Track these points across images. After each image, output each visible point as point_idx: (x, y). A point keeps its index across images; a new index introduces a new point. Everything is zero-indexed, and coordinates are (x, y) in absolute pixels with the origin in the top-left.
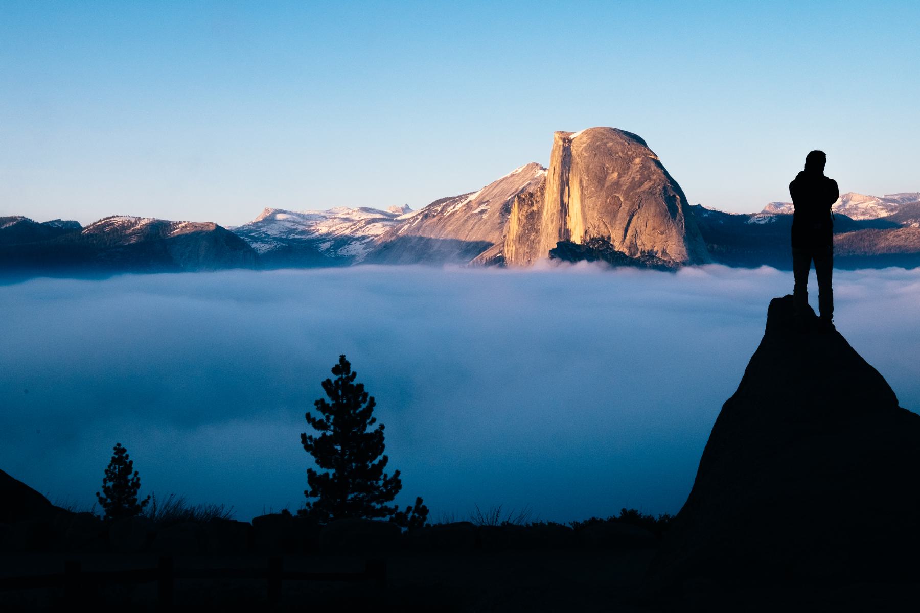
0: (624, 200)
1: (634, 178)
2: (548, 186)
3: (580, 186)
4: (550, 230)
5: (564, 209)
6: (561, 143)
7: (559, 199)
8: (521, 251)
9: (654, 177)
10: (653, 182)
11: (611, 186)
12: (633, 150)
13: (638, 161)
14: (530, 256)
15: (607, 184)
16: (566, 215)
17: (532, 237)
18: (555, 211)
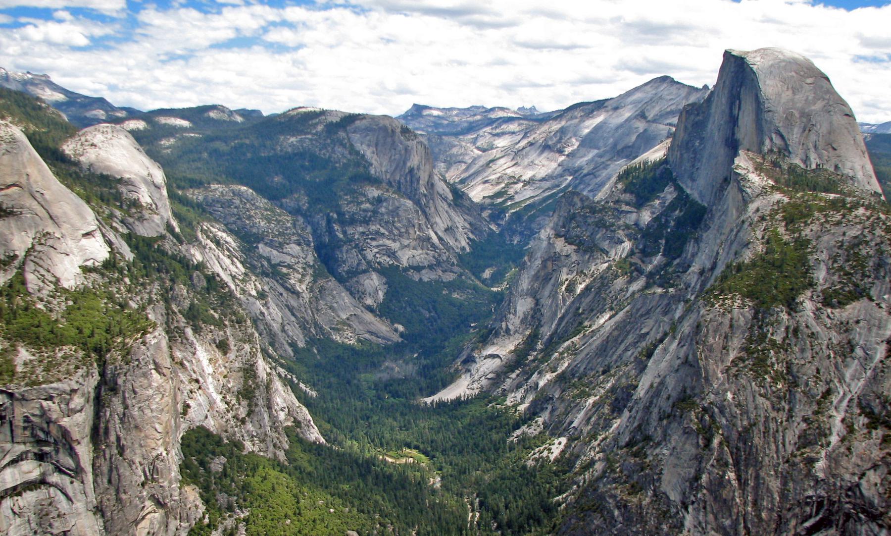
0: (801, 117)
1: (807, 97)
2: (716, 98)
3: (756, 101)
4: (716, 138)
5: (733, 121)
6: (732, 60)
7: (727, 111)
8: (685, 156)
9: (827, 97)
10: (826, 101)
11: (787, 102)
12: (806, 71)
13: (809, 81)
14: (695, 160)
15: (783, 101)
16: (734, 126)
17: (697, 144)
18: (722, 122)
